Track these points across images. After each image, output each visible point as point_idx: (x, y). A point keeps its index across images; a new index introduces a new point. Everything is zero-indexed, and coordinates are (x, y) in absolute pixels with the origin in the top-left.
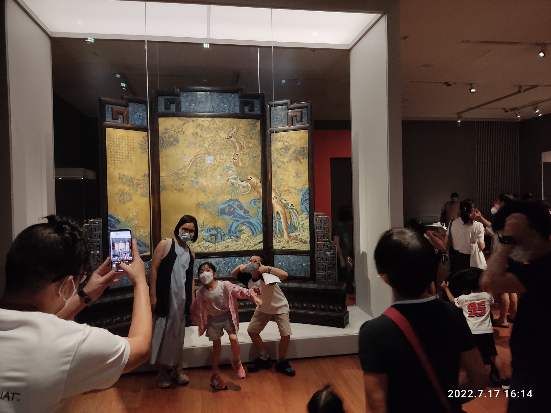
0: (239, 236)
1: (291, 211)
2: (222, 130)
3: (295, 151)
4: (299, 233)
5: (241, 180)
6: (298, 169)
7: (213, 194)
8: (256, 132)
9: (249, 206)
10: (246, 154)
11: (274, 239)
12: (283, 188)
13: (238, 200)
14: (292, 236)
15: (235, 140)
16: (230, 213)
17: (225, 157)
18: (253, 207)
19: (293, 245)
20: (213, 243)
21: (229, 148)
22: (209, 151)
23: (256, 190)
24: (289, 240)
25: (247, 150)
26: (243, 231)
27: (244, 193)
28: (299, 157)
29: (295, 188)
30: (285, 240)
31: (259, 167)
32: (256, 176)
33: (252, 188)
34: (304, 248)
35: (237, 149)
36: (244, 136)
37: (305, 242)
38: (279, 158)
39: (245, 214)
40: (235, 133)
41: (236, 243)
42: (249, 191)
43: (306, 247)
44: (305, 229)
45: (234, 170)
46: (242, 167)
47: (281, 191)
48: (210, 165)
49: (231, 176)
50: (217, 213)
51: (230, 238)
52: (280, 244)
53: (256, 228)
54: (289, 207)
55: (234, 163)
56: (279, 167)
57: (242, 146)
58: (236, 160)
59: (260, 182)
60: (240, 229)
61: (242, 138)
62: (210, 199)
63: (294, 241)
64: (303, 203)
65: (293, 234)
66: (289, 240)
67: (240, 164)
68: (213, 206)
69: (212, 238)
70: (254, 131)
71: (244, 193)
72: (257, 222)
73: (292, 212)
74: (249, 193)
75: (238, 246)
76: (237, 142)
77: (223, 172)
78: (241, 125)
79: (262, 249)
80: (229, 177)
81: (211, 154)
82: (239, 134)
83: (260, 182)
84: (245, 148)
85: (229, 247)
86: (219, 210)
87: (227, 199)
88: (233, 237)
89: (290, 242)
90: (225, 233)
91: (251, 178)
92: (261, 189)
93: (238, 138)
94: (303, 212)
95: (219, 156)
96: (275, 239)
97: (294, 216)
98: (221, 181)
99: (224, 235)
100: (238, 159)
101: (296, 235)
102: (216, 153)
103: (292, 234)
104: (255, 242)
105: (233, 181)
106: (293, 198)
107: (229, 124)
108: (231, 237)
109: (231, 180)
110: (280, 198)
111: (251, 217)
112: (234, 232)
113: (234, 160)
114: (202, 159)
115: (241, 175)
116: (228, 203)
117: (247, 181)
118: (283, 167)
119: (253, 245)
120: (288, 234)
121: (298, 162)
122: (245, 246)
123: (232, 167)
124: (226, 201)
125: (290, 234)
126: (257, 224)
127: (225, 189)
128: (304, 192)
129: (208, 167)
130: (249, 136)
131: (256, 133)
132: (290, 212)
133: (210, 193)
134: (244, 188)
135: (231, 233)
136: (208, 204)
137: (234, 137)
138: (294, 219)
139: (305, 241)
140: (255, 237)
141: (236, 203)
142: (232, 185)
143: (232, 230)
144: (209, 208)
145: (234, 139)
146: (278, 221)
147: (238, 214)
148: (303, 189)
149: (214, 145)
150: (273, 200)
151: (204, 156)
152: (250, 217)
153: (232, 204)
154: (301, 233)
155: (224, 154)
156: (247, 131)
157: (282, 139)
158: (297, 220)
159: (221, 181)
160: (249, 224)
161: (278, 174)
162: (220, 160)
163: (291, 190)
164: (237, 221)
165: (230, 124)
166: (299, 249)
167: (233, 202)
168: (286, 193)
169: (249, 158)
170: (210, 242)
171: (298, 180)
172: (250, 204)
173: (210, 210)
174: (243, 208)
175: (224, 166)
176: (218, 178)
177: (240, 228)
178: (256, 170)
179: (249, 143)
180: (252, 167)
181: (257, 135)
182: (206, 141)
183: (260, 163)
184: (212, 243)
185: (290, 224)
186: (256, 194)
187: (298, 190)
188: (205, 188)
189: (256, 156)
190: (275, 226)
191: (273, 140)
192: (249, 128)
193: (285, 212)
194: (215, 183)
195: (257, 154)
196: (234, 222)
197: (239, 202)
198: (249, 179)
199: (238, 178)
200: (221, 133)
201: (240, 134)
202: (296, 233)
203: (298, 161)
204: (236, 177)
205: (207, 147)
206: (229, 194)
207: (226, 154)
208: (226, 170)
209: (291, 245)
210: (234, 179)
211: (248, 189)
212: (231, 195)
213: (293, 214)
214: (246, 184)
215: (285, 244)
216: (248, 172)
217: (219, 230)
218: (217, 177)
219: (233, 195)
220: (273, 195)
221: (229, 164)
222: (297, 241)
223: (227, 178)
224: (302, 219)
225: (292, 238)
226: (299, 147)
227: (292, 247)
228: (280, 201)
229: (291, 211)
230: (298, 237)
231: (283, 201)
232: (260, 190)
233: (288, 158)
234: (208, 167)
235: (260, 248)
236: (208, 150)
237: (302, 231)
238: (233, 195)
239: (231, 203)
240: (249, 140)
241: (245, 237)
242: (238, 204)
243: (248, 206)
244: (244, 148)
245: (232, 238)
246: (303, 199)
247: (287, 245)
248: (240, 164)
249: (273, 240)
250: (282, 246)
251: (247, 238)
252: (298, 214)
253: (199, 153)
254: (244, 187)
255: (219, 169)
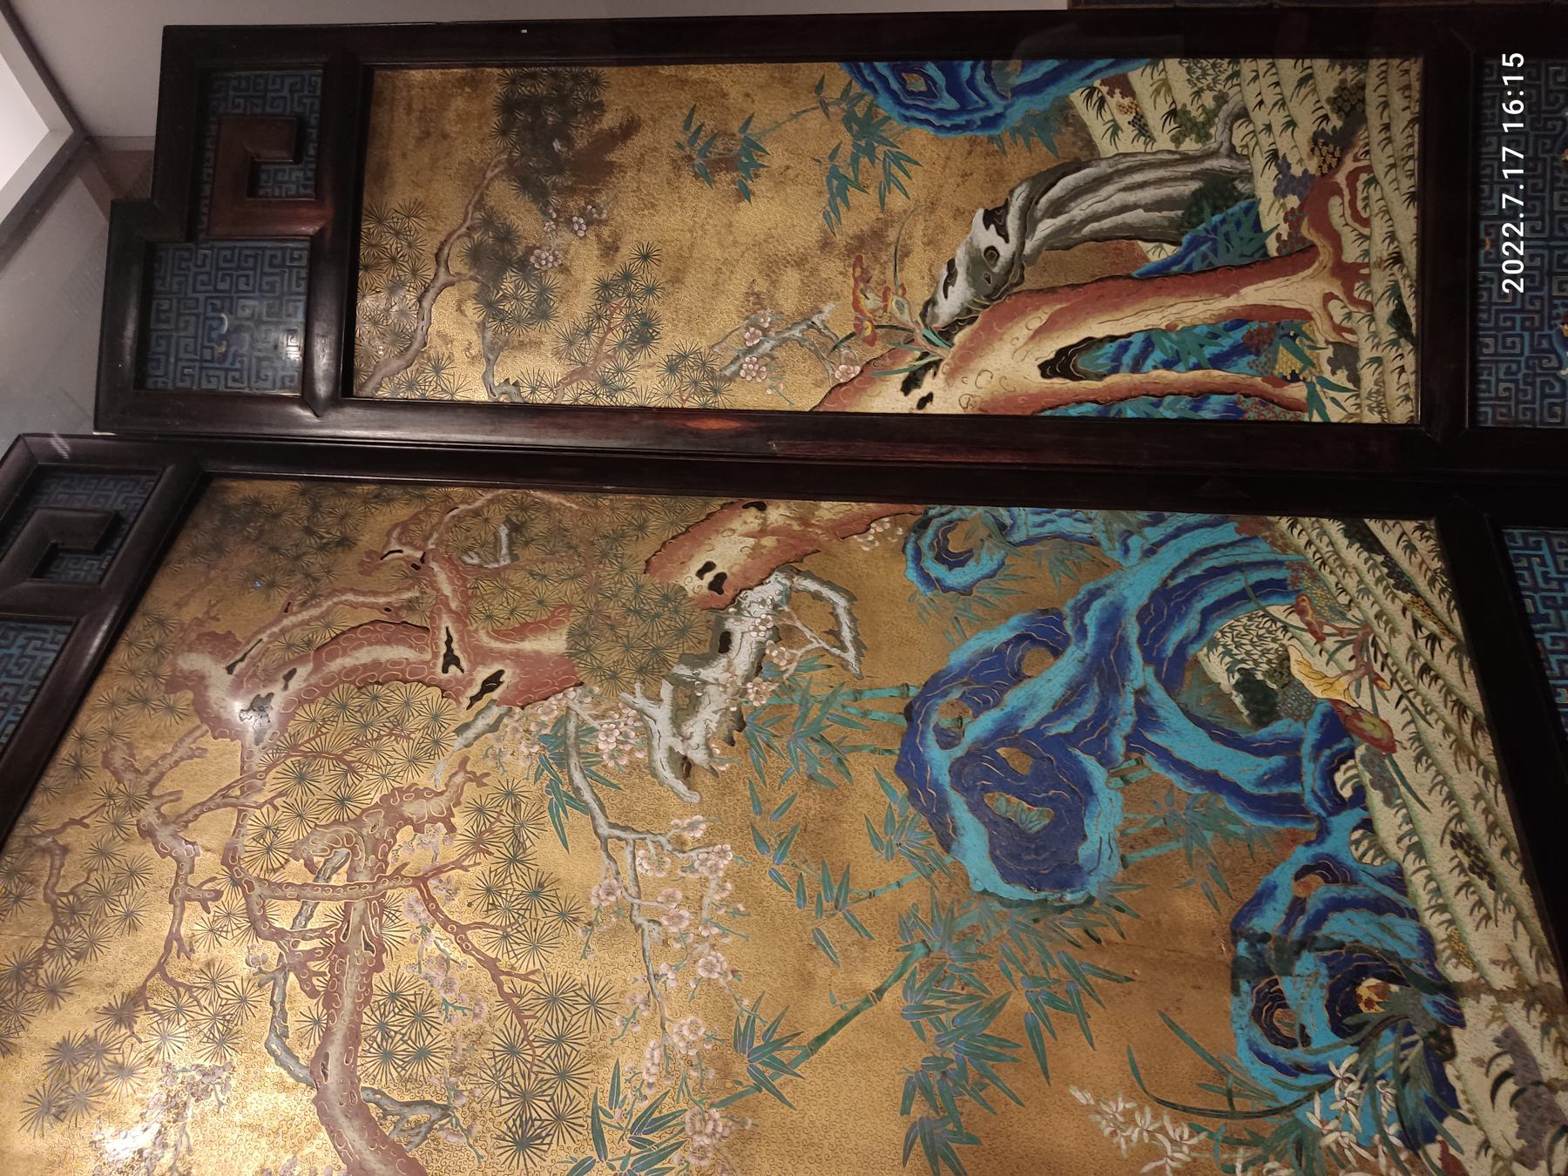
0: (1317, 717)
1: (1045, 227)
2: (152, 785)
3: (531, 185)
4: (1259, 161)
5: (706, 649)
6: (677, 153)
7: (820, 941)
8: (304, 511)
9: (983, 601)
10: (466, 598)
11: (1316, 418)
12: (837, 297)
13: (913, 692)
14: (1284, 229)
15: (303, 671)
16: (1058, 785)
17: (434, 775)
18: (991, 575)
19: (1379, 228)
20: (1460, 1022)
21: (365, 726)
22: (322, 933)
23: (824, 538)
24: (1325, 255)
25: (433, 584)
26: (1259, 676)
27: (847, 635)
28: (581, 144)
29: (839, 186)
30: (1328, 297)
31: (615, 508)
32: (694, 532)
33: (799, 573)
34: (1408, 115)
35: (394, 663)
36: (292, 597)
37: (1349, 104)
38: (566, 327)
39: (1066, 641)
40: (230, 670)
41: (1404, 759)
42: (826, 592)
43: (1398, 101)
44: (1221, 99)
45: (597, 704)
46: (577, 635)
47: (859, 328)
48: (474, 937)
49: (649, 739)
50: (1058, 919)
51: (1355, 815)
52: (1366, 352)
53: (1208, 563)
54: (1006, 250)
55: (528, 696)
56: (644, 334)
57: (384, 617)
58: (501, 673)
59: (761, 507)
60: (1238, 699)
61: (305, 615)
62: (880, 992)
63: (1337, 210)
64: (977, 117)
65: (1272, 217)
66: (1325, 255)
67: (553, 644)
68: (968, 957)
69: (1387, 1022)
70: (286, 517)
71: (847, 635)
72: (1151, 551)
73: (1060, 220)
74: (851, 598)
75: (1434, 734)
76: (332, 656)
77: (586, 809)
78: (193, 610)
79: (1432, 525)
80: (660, 756)
81: (354, 918)
82: (264, 637)
83: (753, 511)
84: (407, 595)
85: (1462, 829)
86: (1017, 892)
87: (891, 793)
88: (1339, 778)
89: (1351, 254)
90: (1302, 855)
91: (700, 574)
92: (825, 504)
93: (289, 646)
94: (1064, 109)
95: (405, 834)
96: (1314, 400)
97: (1100, 207)
98: (680, 845)
99: (1329, 869)
100: (502, 656)
101: (1280, 192)
102: (364, 860)
103: (1267, 225)
104: (1370, 579)
105: (707, 719)
106: (932, 206)
107: (132, 708)
108: (1340, 805)
109: (697, 739)
110: (920, 331)
111: (1095, 595)
112: (1277, 761)
113: (495, 695)
114: (382, 1027)
115: (656, 650)
116: (937, 787)
117: (734, 601)
118: (650, 290)
119: (1407, 597)
120: (1261, 265)
121: (619, 155)
122: (1426, 669)
123: (561, 722)
124: (924, 811)
125: (1272, 246)
126: (1170, 557)
127: (781, 810)
128: (885, 106)
129: (490, 964)
130: (315, 562)
131: (315, 508)
132: (1061, 241)
133: (806, 980)
134: (791, 629)
135: (1297, 799)
136: (939, 1024)
137: (269, 679)
138: (1125, 209)
139: (1331, 101)
140: (1315, 578)
141: (940, 716)
142: (750, 738)
143: (1261, 782)
144: (993, 1010)
145: (292, 673)
146: (1136, 367)
147: (1063, 708)
148: (860, 111)
149: (274, 878)
150: (931, 409)
151: (347, 1003)
152: (1097, 605)
153: (959, 752)
154: (1265, 140)
155: (409, 778)
156: (259, 570)
157: (411, 297)
158: (1138, 177)
159: (688, 836)
160: (1178, 614)
161: (704, 345)
162: (452, 829)
163: (852, 230)
164: (1146, 716)
165: (132, 699)
166: (1411, 165)
167: (931, 737)
168: (875, 273)
169: (517, 578)
170: (1441, 1049)
171: (776, 156)
172: (966, 591)
173: (1019, 1002)
174: (999, 651)
175: (530, 789)
176: (644, 867)
177: (1227, 697)
178: (641, 528)
179: (376, 558)
180: (604, 555)
181: (326, 505)
182: (201, 954)
183: (582, 497)
184: (1457, 1033)
185: (1169, 250)
186: (863, 545)
187: (864, 161)
188: (741, 1039)
189: (508, 521)
190: (1185, 402)
191: (411, 385)
192: (244, 558)
193: (1052, 290)
194: (697, 905)
195: (497, 515)
196: (1164, 755)
197: (936, 685)
198: (718, 584)
199: (683, 671)
200: (176, 796)
201: (261, 630)
202: (1265, 183)
203: (612, 157)
204: (666, 690)
205: (270, 951)
206: (835, 777)
207: (413, 761)
208: (578, 777)
209: (1381, 249)
210: (685, 707)
211: (808, 601)
212: (851, 758)
213: (1078, 211)
214: (761, 612)
215: (1370, 307)
216: (639, 588)
217: (1269, 920)
218: (628, 880)
219: (858, 737)
220: (888, 399)
221: (523, 749)
222: (1341, 178)
223: (667, 774)
224: (1128, 132)
225: (1306, 231)
226: (500, 143)
227: (1392, 237)
228: (947, 333)
229: (1045, 227)
230: (1297, 171)
231: (948, 308)
232: (829, 510)
233: (576, 243)
234: (490, 964)
235: (1425, 547)
236: (304, 946)
237: (1240, 132)
238: (858, 737)
239: (939, 760)
240: (349, 562)
241: (1319, 662)
242: (955, 695)
243: (979, 611)
244: (410, 606)
245: (1360, 796)
246: (943, 113)
247: (1380, 282)
248: (553, 644)
249: (1327, 425)
250: (1388, 333)
251: (1330, 643)
252: (1077, 166)
253: (305, 1054)
254: (782, 634)
255: (545, 849)
